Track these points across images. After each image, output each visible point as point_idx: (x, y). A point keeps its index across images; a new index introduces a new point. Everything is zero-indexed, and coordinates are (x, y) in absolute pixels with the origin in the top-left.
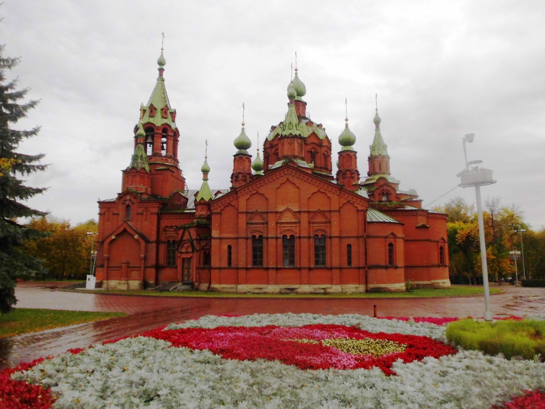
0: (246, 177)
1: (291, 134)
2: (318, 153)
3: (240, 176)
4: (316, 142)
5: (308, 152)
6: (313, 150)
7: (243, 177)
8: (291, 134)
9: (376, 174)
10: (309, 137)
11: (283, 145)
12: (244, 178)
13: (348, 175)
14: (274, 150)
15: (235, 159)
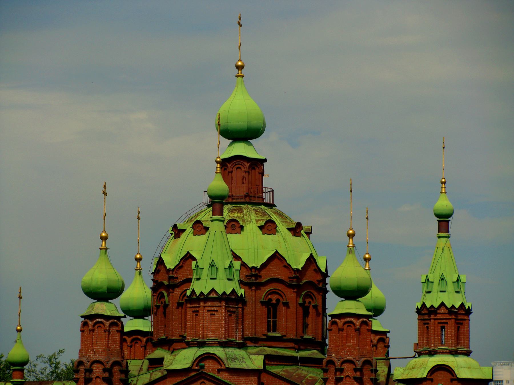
0: (109, 371)
1: (213, 290)
2: (286, 305)
3: (97, 369)
4: (284, 276)
5: (263, 303)
6: (274, 298)
7: (105, 370)
8: (213, 290)
9: (431, 353)
10: (264, 266)
11: (196, 312)
12: (106, 375)
13: (346, 373)
14: (178, 291)
15: (85, 324)
